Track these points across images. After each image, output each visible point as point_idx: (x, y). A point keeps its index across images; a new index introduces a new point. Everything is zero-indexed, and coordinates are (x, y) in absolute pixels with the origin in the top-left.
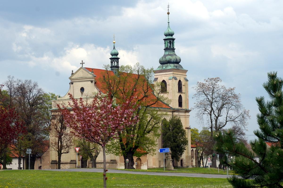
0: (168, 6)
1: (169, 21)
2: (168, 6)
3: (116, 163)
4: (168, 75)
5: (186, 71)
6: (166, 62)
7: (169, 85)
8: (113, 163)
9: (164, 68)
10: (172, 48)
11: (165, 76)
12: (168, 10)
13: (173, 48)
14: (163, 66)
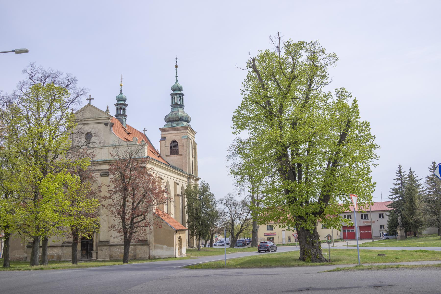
0: (177, 58)
1: (177, 74)
2: (177, 58)
3: (149, 245)
4: (181, 134)
6: (176, 119)
7: (183, 145)
8: (143, 245)
9: (175, 125)
10: (182, 104)
11: (176, 135)
13: (183, 104)
14: (173, 123)
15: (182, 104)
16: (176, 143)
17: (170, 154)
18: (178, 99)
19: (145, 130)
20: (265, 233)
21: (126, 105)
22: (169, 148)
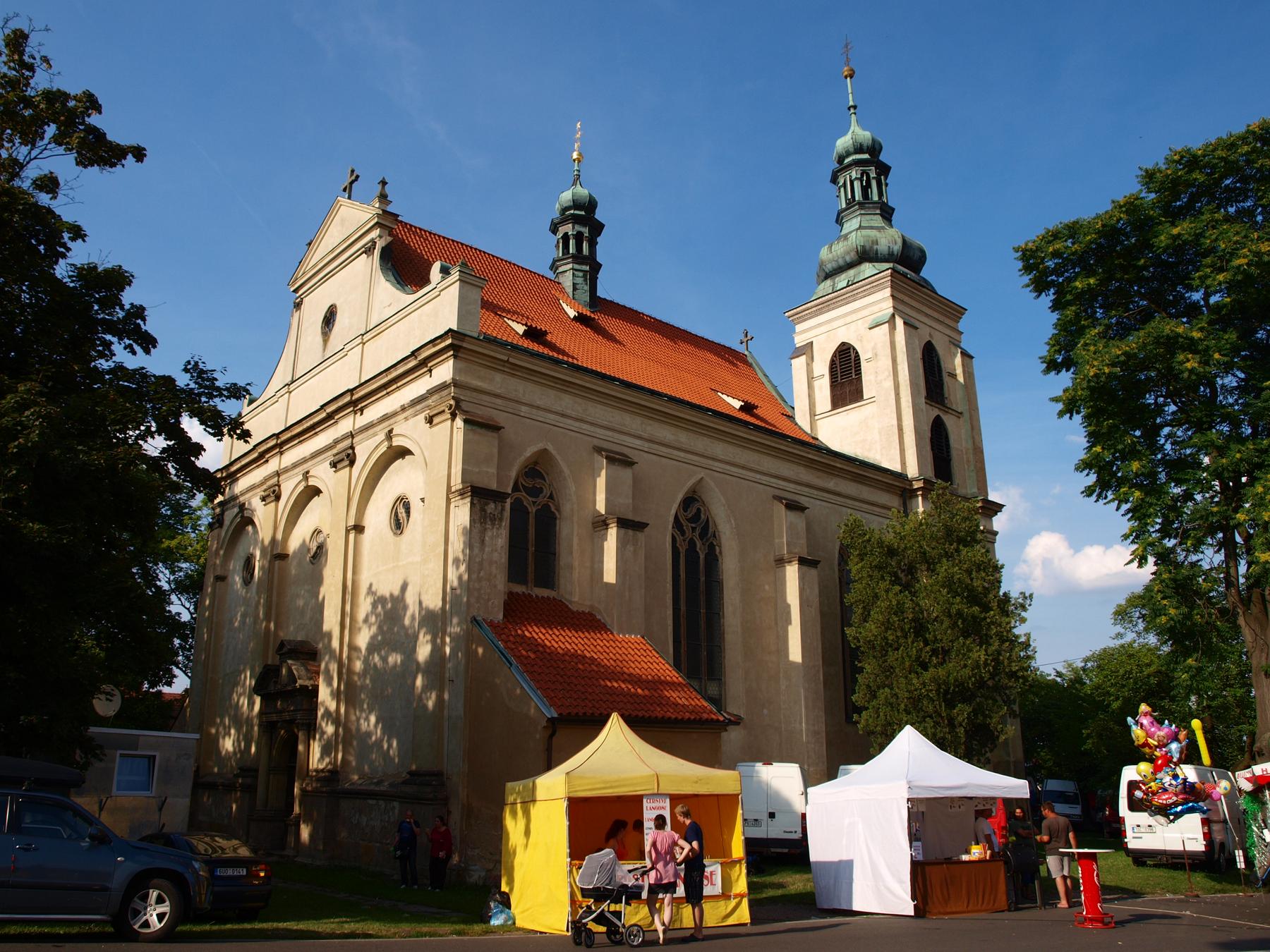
5: (956, 311)
6: (848, 259)
11: (849, 319)
16: (853, 356)
17: (830, 408)
18: (857, 185)
19: (747, 338)
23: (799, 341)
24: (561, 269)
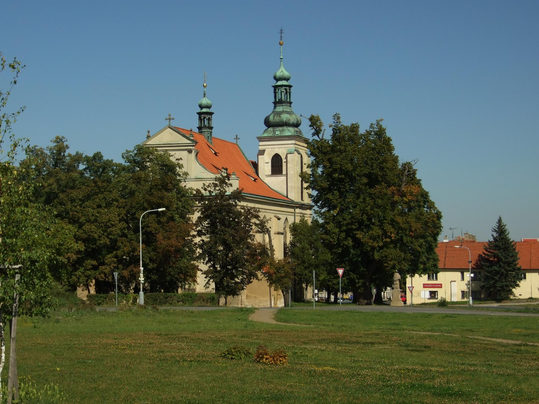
0: (281, 30)
2: (281, 30)
10: (288, 100)
12: (281, 37)
15: (288, 100)
17: (270, 173)
20: (424, 284)
21: (211, 114)
22: (270, 165)
23: (261, 148)
24: (203, 130)
